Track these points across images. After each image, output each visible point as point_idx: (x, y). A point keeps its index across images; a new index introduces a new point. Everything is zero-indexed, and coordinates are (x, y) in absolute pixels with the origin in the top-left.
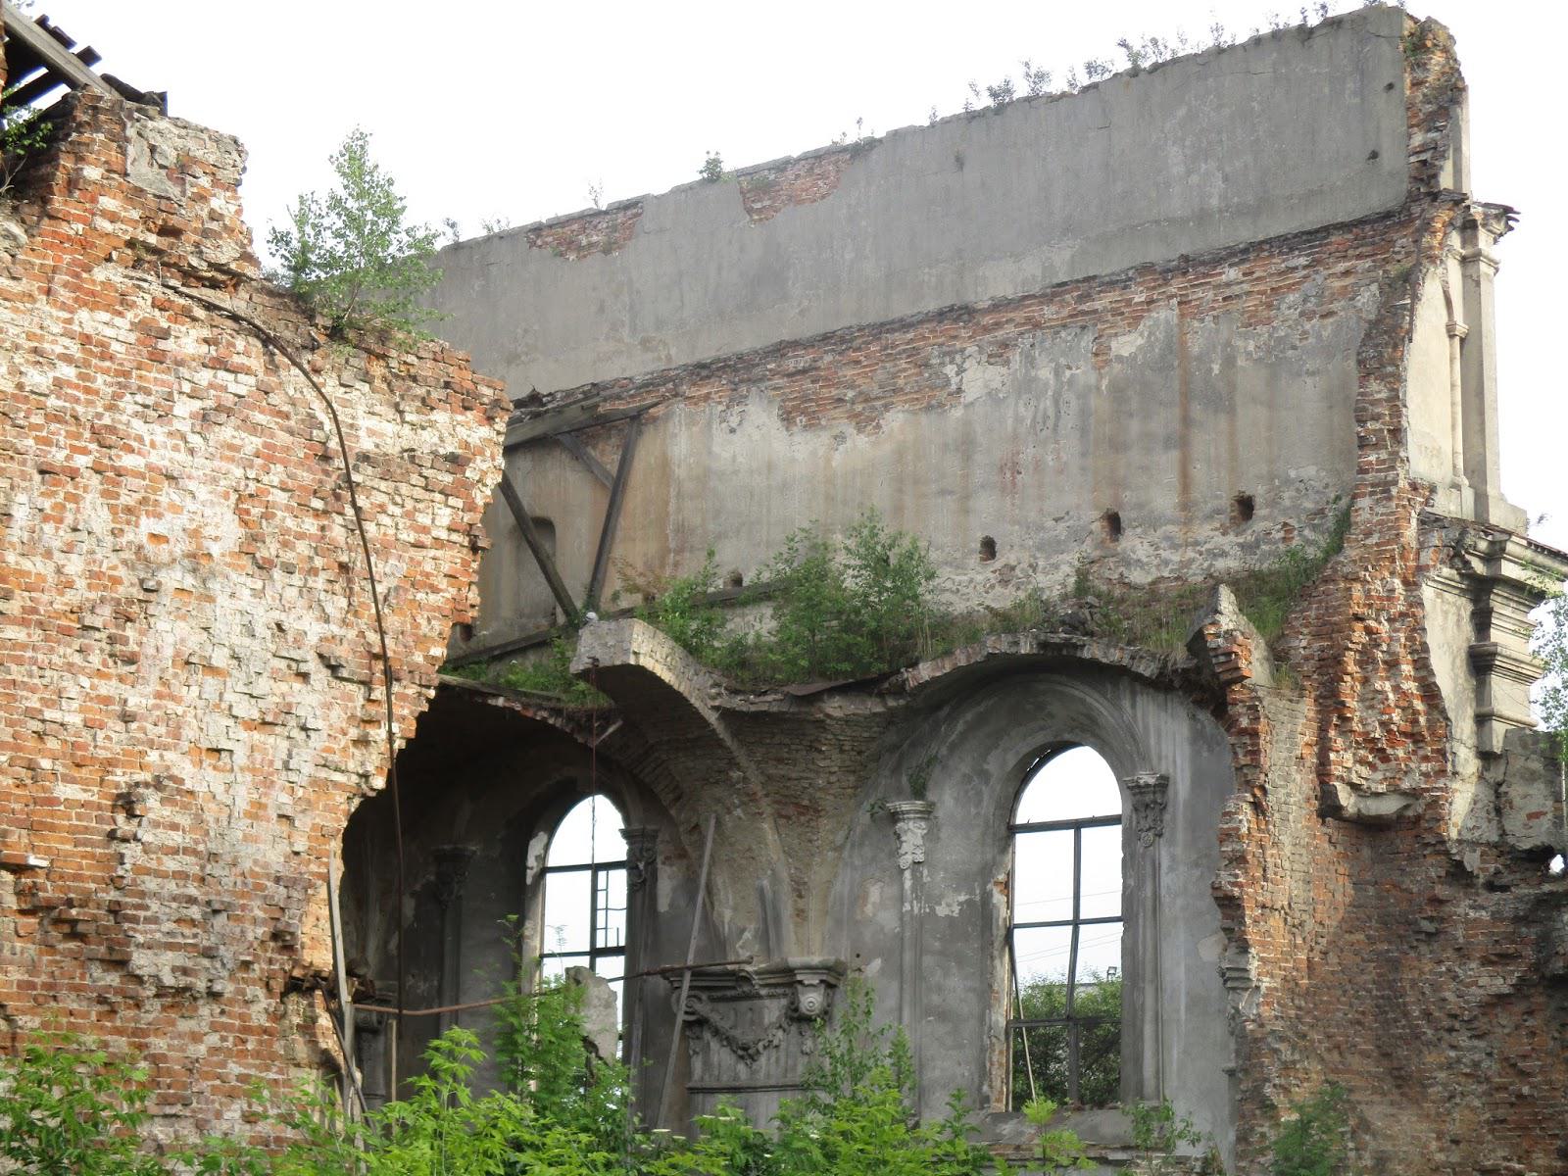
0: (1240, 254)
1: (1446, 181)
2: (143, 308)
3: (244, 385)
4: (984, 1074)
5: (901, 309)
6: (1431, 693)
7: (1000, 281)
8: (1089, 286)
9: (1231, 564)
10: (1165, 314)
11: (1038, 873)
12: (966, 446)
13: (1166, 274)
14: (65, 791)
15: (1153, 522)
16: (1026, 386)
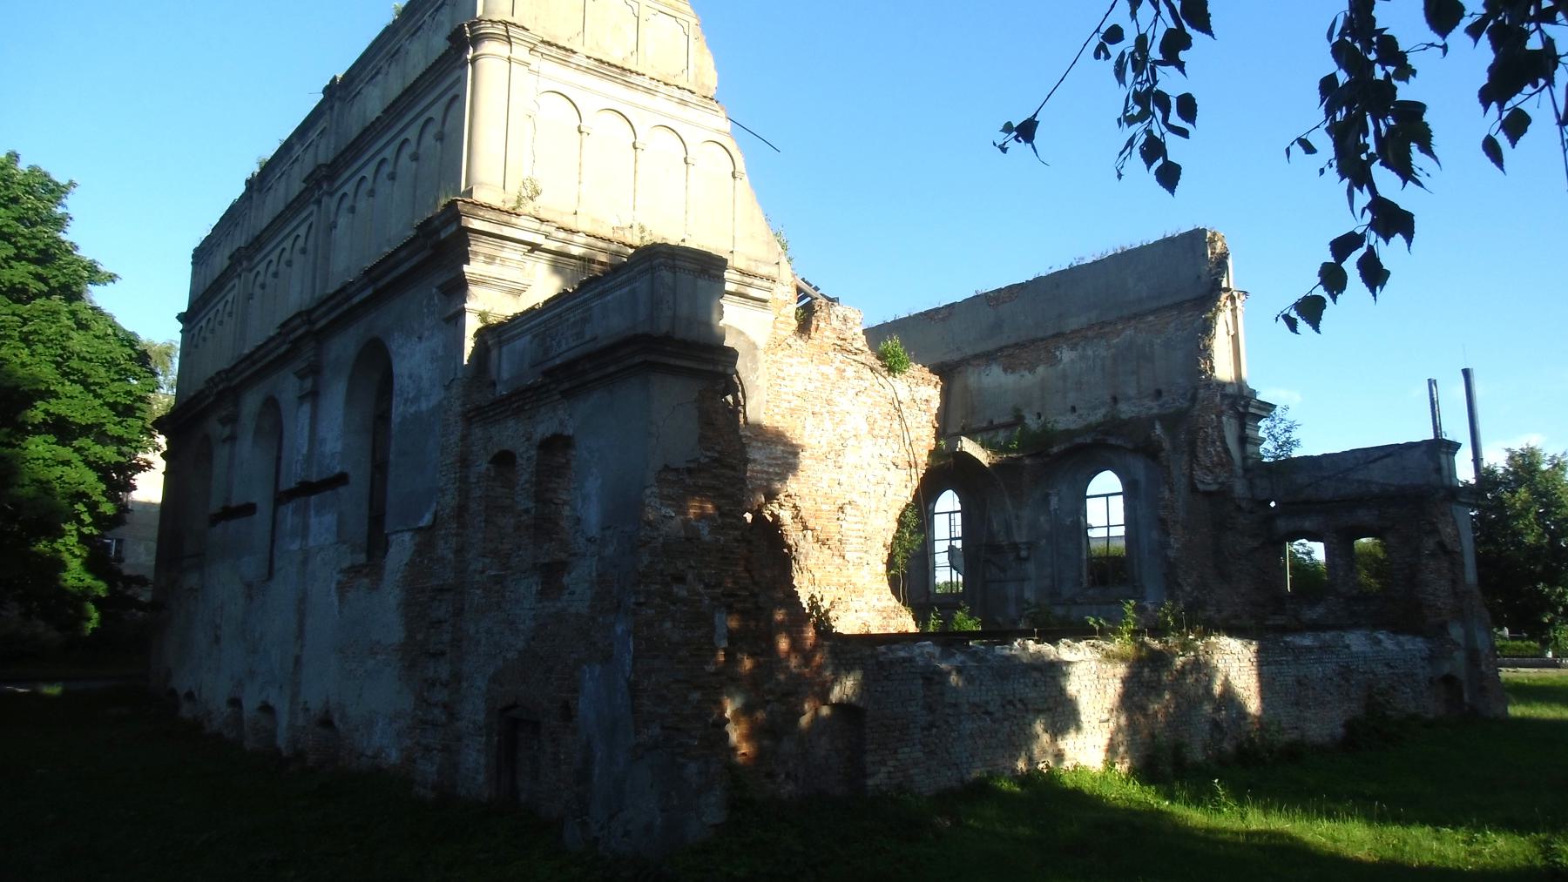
0: (1152, 312)
1: (1224, 285)
2: (837, 364)
3: (867, 384)
4: (1081, 575)
5: (1041, 335)
6: (1227, 450)
7: (1073, 324)
8: (1103, 324)
9: (1155, 411)
10: (1129, 332)
11: (1095, 513)
12: (1064, 377)
13: (1129, 319)
14: (824, 507)
15: (1129, 399)
16: (1083, 357)
